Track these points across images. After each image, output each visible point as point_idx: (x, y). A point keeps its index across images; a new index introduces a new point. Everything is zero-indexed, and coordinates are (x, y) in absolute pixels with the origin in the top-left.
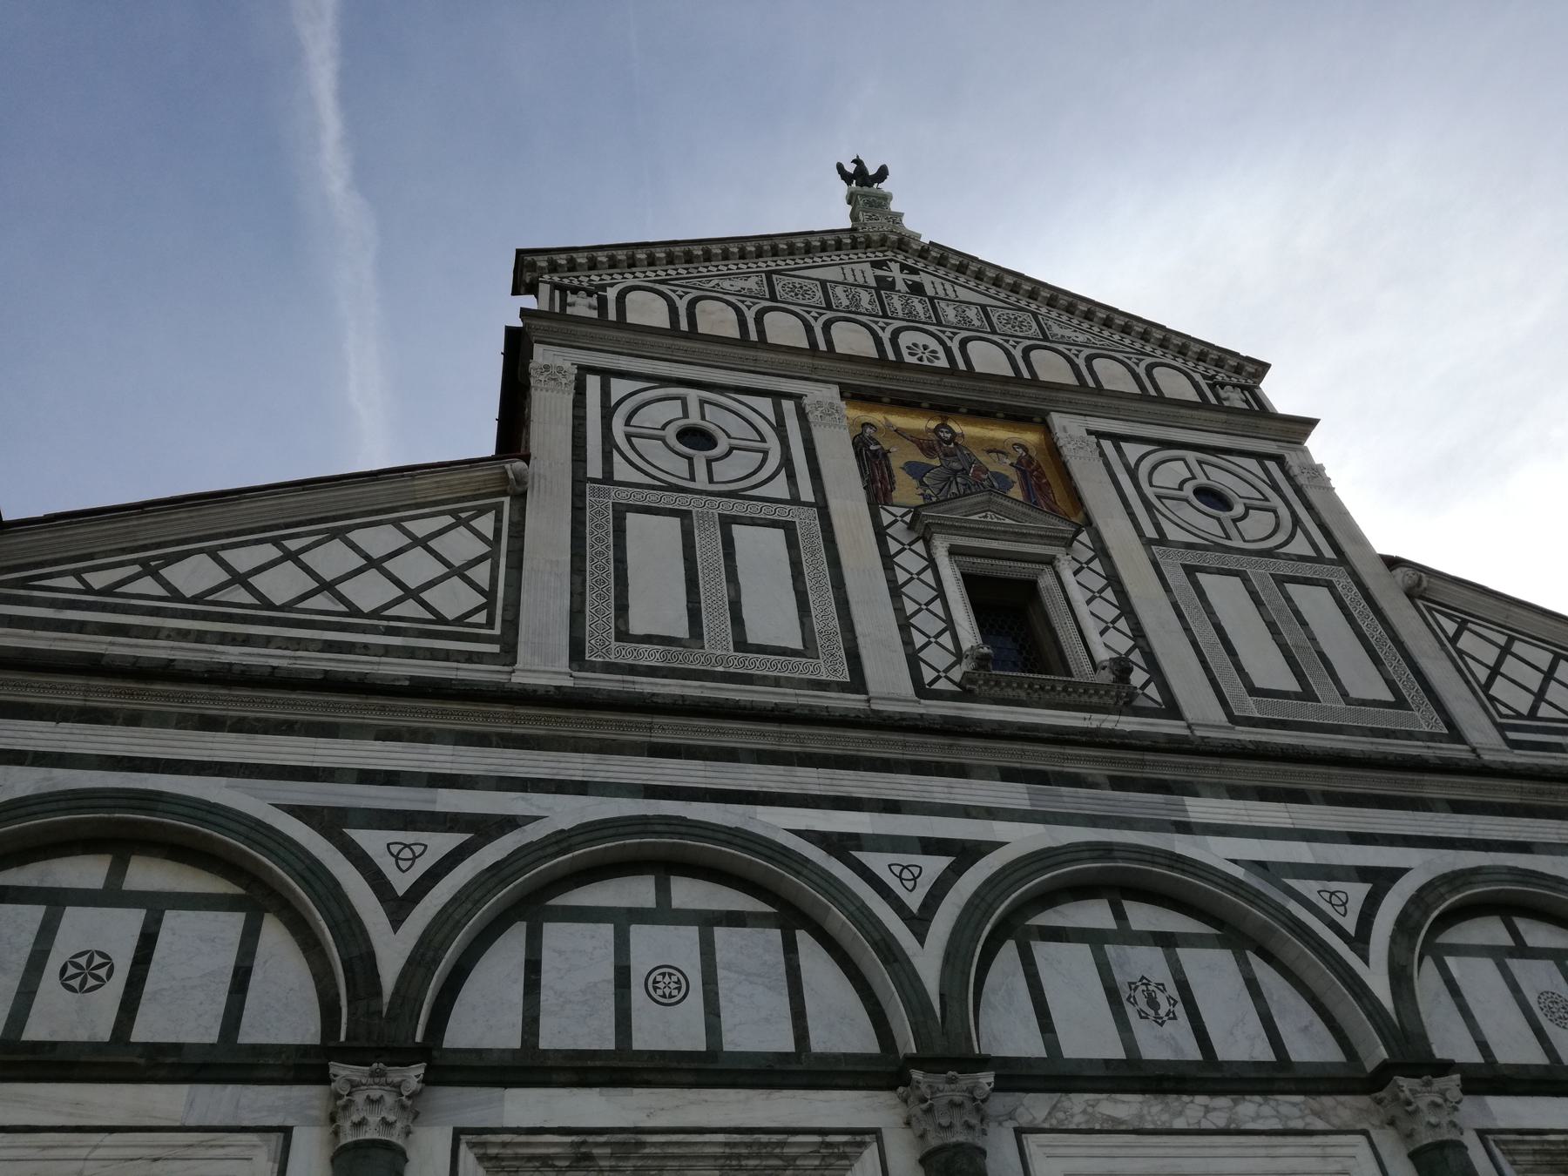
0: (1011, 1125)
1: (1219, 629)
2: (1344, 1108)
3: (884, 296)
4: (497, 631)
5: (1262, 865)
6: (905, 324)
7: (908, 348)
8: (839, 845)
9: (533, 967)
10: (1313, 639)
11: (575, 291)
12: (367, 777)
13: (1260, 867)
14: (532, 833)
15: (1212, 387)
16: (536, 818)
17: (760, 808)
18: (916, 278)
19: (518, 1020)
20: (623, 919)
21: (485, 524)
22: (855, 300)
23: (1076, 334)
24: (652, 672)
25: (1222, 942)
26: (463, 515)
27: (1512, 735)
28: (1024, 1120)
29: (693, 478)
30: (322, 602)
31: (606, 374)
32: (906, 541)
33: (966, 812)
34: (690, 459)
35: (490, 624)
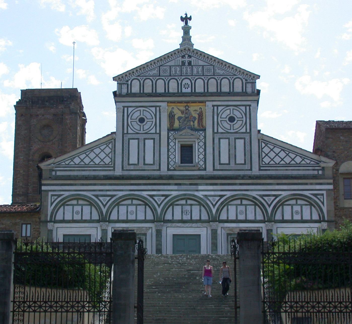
0: (166, 226)
1: (219, 152)
2: (205, 225)
3: (182, 68)
4: (113, 165)
5: (206, 195)
6: (184, 77)
7: (184, 85)
8: (151, 196)
9: (118, 211)
10: (235, 152)
11: (124, 84)
12: (100, 190)
13: (206, 196)
14: (117, 197)
15: (246, 83)
16: (118, 195)
17: (143, 192)
18: (190, 59)
19: (117, 217)
20: (127, 205)
21: (110, 146)
22: (176, 71)
23: (221, 71)
24: (132, 170)
25: (198, 205)
26: (107, 144)
27: (262, 168)
28: (167, 226)
29: (140, 130)
30: (92, 163)
31: (128, 107)
32: (172, 139)
33: (169, 190)
34: (140, 126)
35: (112, 164)
